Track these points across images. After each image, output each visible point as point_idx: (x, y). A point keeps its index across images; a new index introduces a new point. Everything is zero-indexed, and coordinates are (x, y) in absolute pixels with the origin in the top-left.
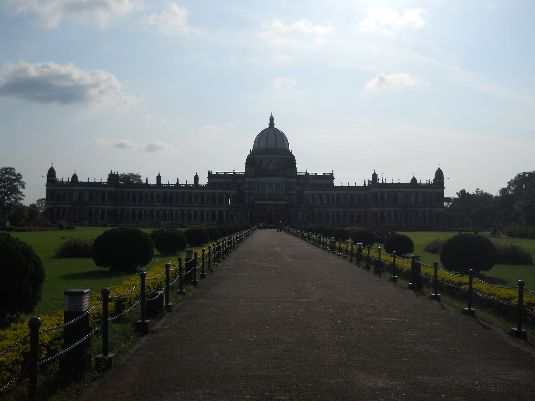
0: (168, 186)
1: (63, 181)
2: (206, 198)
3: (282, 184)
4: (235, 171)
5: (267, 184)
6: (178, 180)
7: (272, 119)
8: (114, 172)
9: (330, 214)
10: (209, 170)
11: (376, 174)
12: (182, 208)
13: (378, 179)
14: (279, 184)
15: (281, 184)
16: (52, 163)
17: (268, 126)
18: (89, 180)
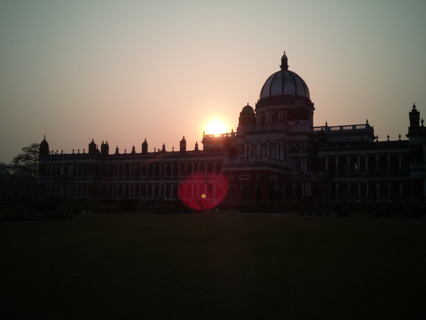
0: (155, 155)
1: (57, 154)
2: (193, 168)
3: (280, 143)
4: (233, 132)
5: (259, 144)
6: (164, 146)
7: (284, 60)
8: (103, 142)
9: (359, 185)
10: (204, 133)
11: (418, 111)
12: (168, 181)
13: (420, 120)
14: (276, 143)
15: (278, 144)
16: (45, 136)
17: (280, 69)
18: (85, 151)
